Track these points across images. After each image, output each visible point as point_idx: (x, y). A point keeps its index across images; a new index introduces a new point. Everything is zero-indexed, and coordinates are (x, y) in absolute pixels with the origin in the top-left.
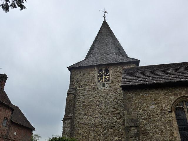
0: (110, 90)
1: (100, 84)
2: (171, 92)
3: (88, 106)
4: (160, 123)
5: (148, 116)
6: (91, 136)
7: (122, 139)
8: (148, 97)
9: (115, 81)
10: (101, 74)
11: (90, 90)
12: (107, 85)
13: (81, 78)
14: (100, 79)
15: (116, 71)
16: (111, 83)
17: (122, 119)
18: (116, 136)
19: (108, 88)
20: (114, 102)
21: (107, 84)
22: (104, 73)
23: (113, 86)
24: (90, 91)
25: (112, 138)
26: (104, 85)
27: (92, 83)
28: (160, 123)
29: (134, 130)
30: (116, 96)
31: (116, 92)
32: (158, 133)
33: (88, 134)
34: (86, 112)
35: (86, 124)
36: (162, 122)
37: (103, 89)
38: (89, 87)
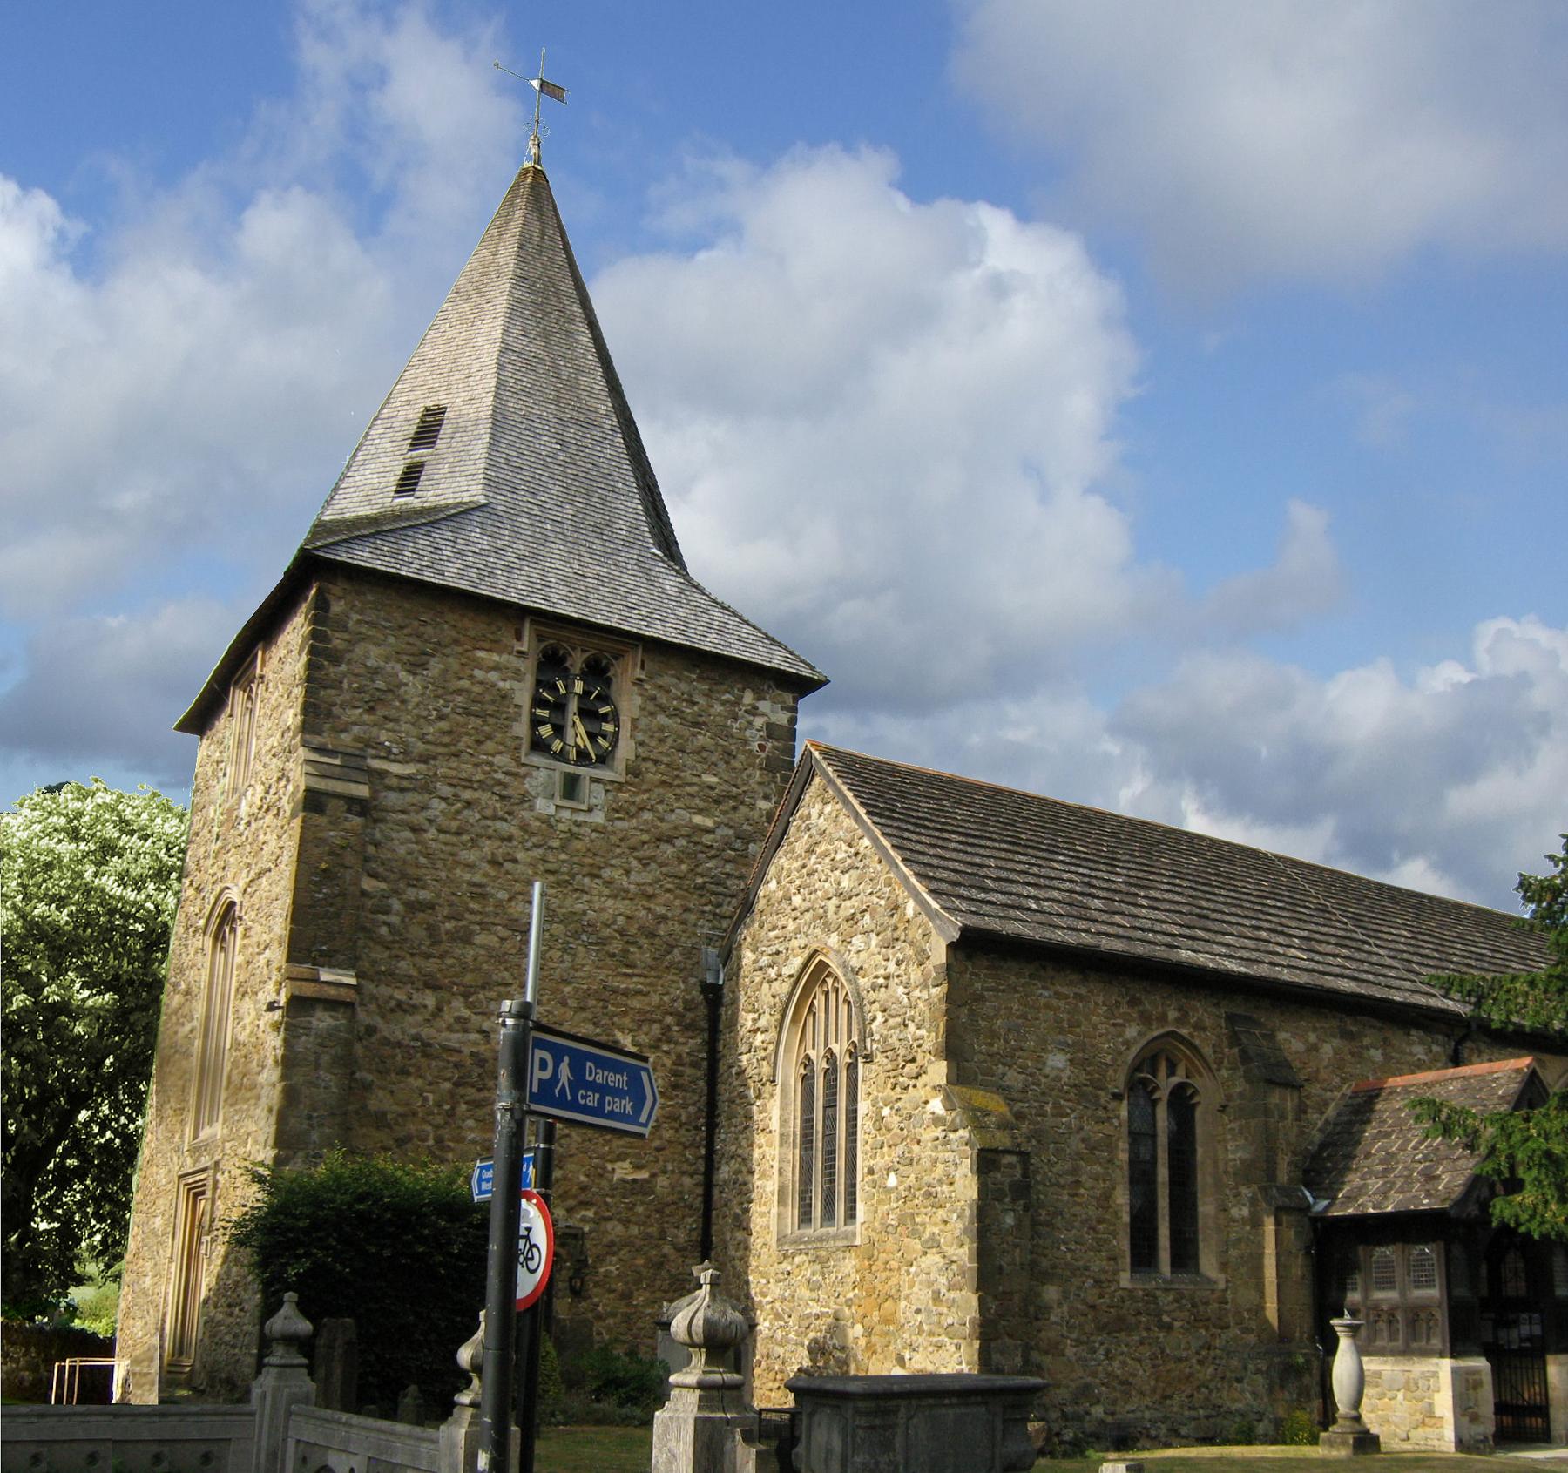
0: (614, 839)
1: (544, 774)
2: (1133, 1002)
3: (449, 918)
4: (1075, 1144)
5: (1036, 1104)
6: (460, 1139)
7: (653, 1175)
8: (1048, 1006)
9: (652, 777)
10: (562, 691)
11: (467, 795)
12: (594, 795)
13: (403, 676)
14: (546, 731)
15: (663, 699)
16: (620, 787)
17: (667, 1053)
18: (621, 1158)
19: (598, 818)
20: (633, 931)
21: (594, 780)
22: (579, 687)
23: (633, 809)
24: (468, 804)
25: (596, 1167)
26: (571, 786)
27: (490, 746)
28: (1075, 1144)
29: (1011, 1166)
30: (650, 890)
31: (652, 858)
32: (1063, 1187)
33: (437, 1127)
34: (430, 966)
35: (426, 1055)
36: (1083, 1140)
37: (566, 814)
38: (467, 770)
